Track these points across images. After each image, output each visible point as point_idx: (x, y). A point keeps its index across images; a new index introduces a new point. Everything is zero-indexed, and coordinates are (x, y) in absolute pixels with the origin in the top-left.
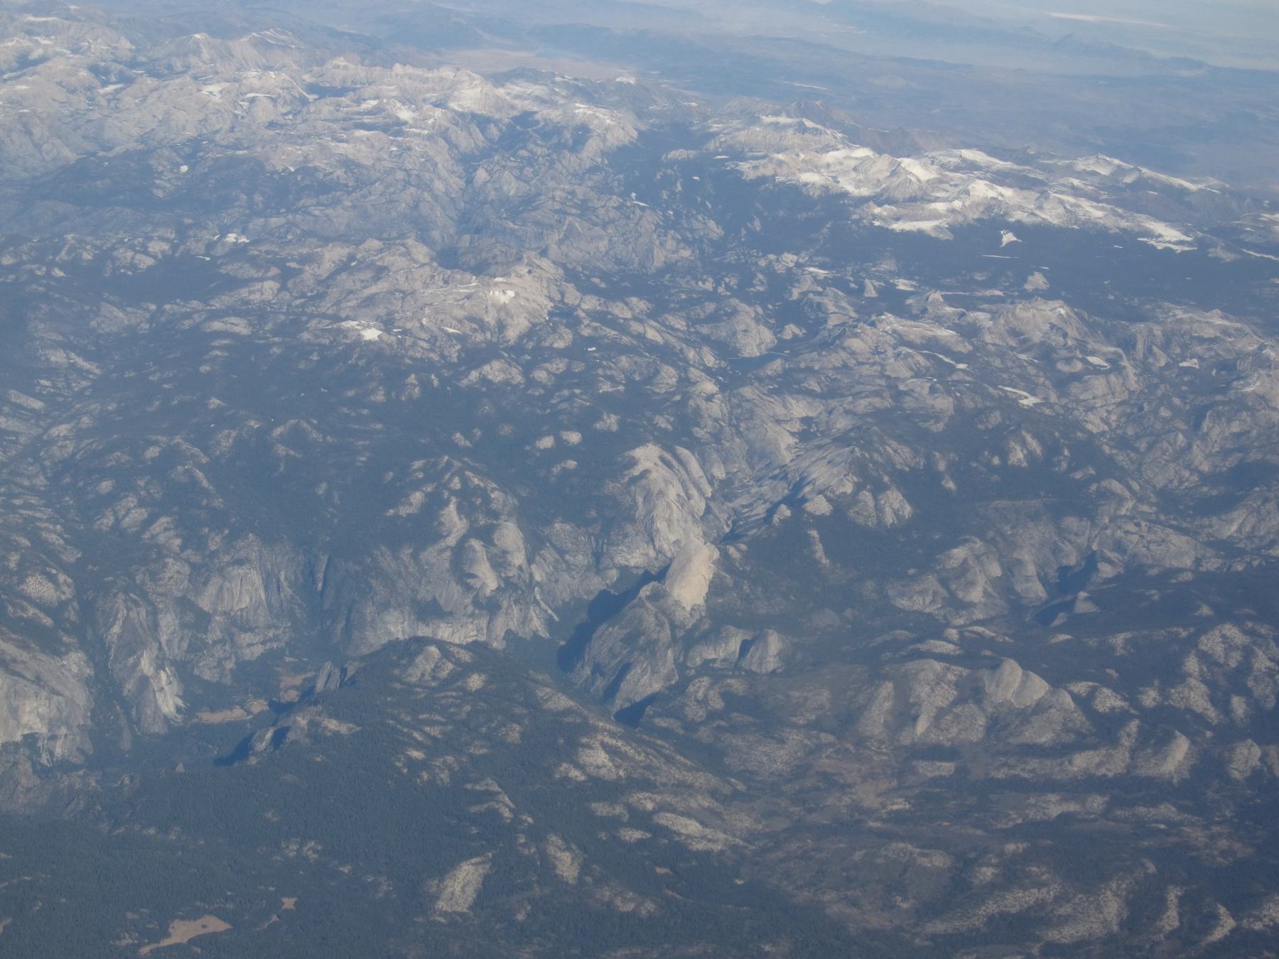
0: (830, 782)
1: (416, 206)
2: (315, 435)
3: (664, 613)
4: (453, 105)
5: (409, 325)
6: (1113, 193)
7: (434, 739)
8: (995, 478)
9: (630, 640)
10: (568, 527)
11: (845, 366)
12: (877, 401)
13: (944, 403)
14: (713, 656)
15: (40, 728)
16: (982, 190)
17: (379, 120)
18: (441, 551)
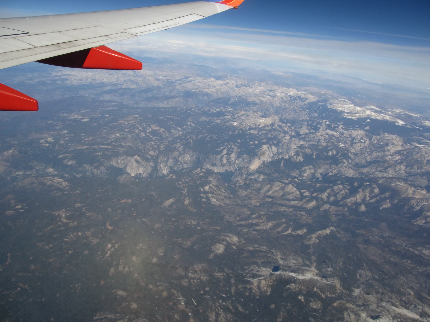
0: (250, 199)
1: (267, 108)
2: (215, 137)
3: (247, 170)
4: (288, 94)
5: (243, 123)
6: (399, 116)
7: (186, 181)
8: (324, 157)
9: (239, 173)
10: (246, 155)
11: (314, 137)
12: (314, 143)
13: (324, 144)
14: (252, 178)
15: (142, 172)
16: (368, 112)
17: (273, 95)
18: (220, 156)
